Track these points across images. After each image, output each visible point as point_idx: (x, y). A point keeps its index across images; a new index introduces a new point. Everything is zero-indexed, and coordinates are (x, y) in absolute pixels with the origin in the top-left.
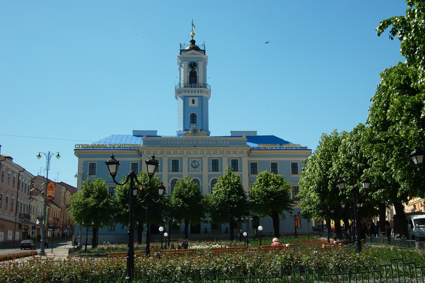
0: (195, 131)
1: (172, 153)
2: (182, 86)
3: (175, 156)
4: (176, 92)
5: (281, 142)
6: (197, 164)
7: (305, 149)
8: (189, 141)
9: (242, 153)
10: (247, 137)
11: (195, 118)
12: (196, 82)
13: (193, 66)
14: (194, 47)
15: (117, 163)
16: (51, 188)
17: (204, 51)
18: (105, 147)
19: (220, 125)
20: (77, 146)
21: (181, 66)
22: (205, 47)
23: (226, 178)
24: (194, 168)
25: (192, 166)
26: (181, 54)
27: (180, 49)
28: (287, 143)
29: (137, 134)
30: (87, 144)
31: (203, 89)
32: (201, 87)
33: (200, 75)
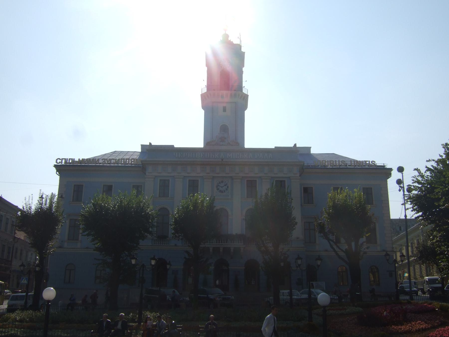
20: (59, 161)
22: (241, 41)
24: (221, 192)
25: (218, 189)
30: (73, 158)
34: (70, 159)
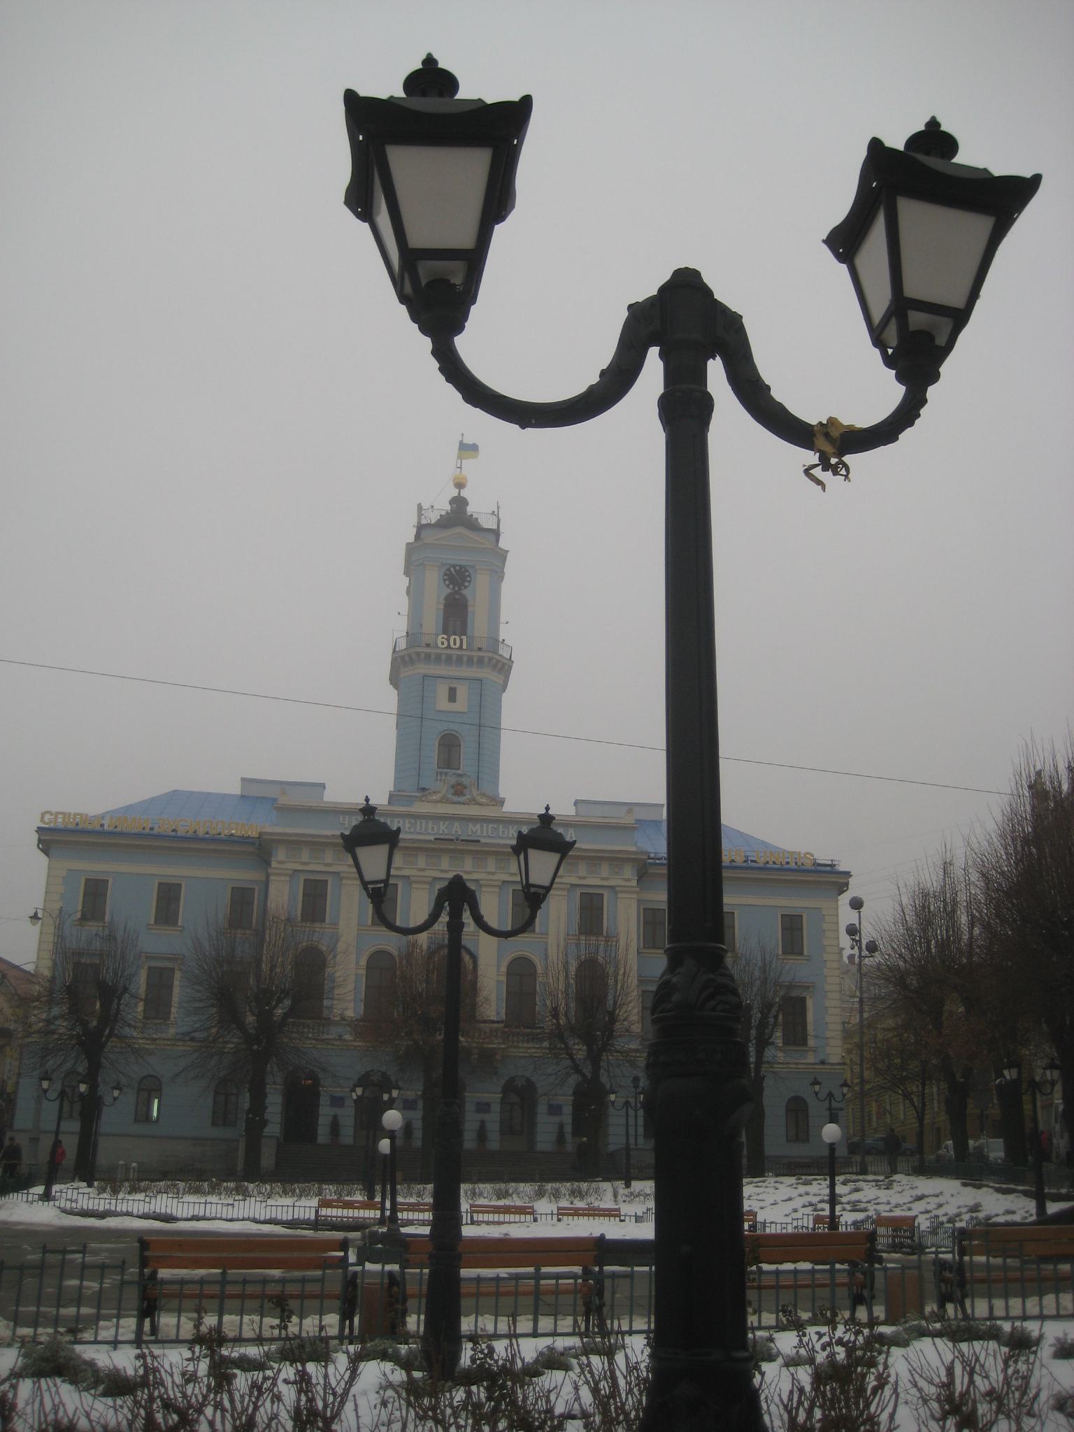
0: (459, 790)
4: (394, 660)
12: (463, 632)
13: (458, 578)
17: (496, 533)
20: (47, 817)
26: (418, 537)
27: (414, 521)
32: (480, 649)
34: (75, 815)
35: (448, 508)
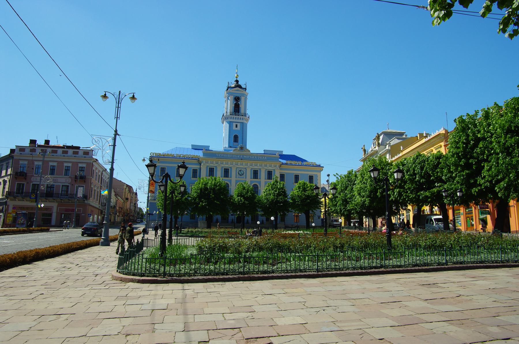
0: (242, 148)
1: (224, 163)
2: (229, 114)
3: (227, 166)
5: (303, 160)
6: (242, 173)
7: (319, 166)
8: (237, 155)
9: (276, 166)
10: (280, 155)
11: (237, 139)
12: (239, 112)
13: (237, 99)
14: (238, 86)
15: (186, 168)
16: (152, 184)
17: (246, 89)
18: (173, 157)
19: (255, 145)
21: (228, 99)
23: (273, 184)
24: (240, 175)
26: (227, 90)
28: (305, 161)
29: (195, 148)
31: (244, 117)
33: (242, 106)
35: (235, 83)
